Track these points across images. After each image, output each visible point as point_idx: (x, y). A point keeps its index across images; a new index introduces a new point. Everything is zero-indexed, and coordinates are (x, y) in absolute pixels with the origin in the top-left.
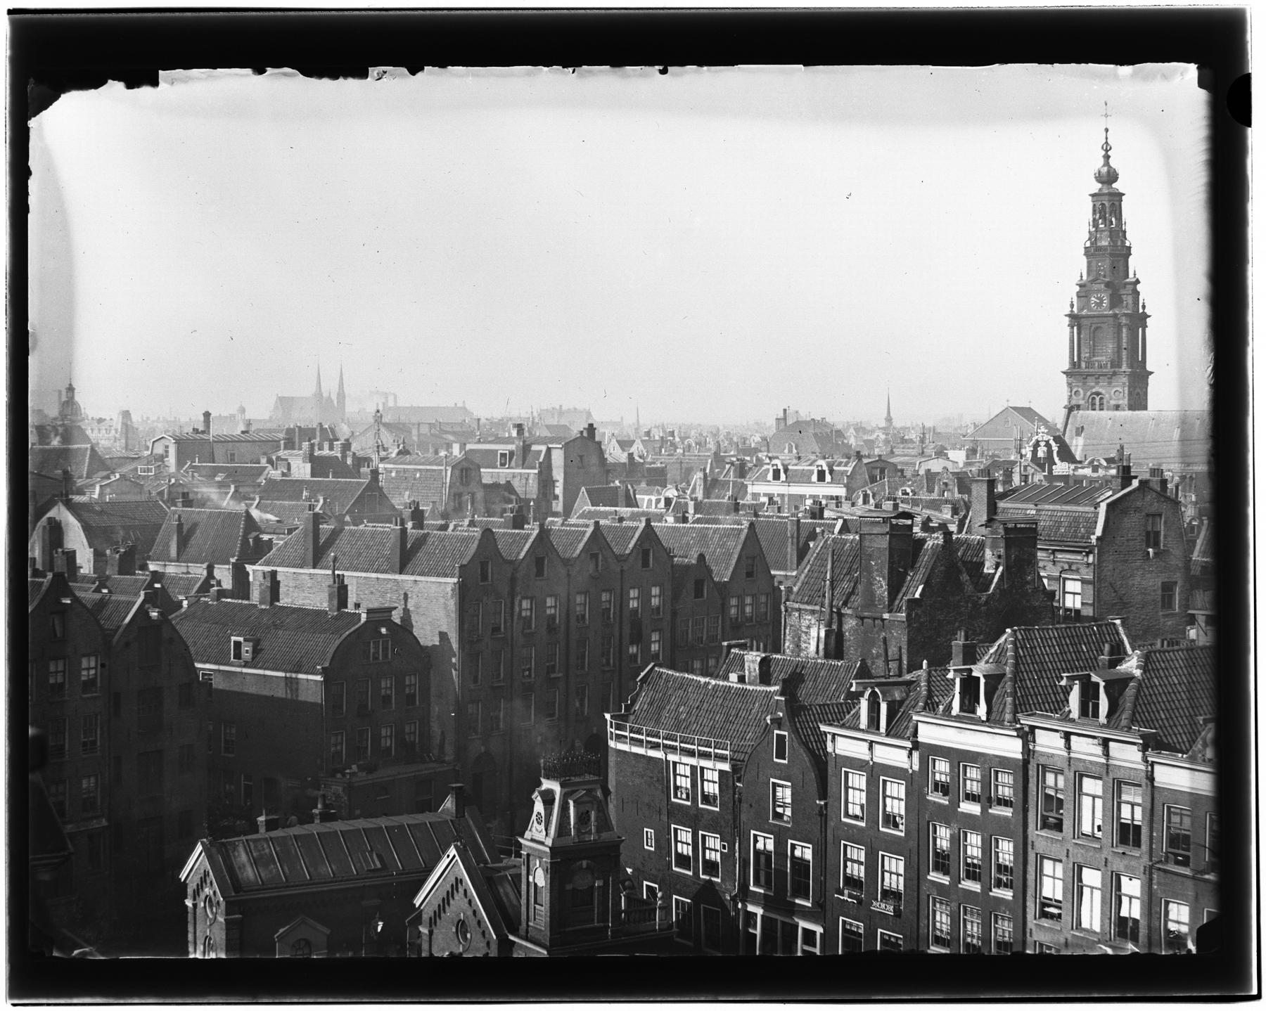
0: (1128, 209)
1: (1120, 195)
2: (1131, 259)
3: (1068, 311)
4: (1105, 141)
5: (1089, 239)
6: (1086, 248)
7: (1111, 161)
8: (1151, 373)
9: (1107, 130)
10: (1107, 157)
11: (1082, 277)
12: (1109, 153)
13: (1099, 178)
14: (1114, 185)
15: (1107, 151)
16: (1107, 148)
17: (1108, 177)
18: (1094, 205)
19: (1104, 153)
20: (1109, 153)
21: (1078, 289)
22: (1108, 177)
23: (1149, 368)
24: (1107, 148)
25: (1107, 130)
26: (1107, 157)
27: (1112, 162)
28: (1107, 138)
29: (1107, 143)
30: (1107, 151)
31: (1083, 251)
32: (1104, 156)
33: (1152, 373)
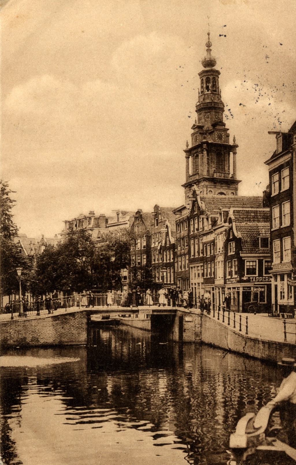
1: (218, 73)
3: (185, 148)
4: (207, 41)
5: (199, 102)
7: (212, 52)
9: (209, 34)
10: (209, 50)
11: (196, 122)
12: (211, 48)
14: (213, 68)
16: (209, 45)
17: (209, 63)
18: (202, 79)
21: (192, 131)
22: (209, 63)
24: (209, 45)
25: (209, 34)
26: (209, 50)
28: (209, 39)
29: (209, 42)
32: (207, 50)
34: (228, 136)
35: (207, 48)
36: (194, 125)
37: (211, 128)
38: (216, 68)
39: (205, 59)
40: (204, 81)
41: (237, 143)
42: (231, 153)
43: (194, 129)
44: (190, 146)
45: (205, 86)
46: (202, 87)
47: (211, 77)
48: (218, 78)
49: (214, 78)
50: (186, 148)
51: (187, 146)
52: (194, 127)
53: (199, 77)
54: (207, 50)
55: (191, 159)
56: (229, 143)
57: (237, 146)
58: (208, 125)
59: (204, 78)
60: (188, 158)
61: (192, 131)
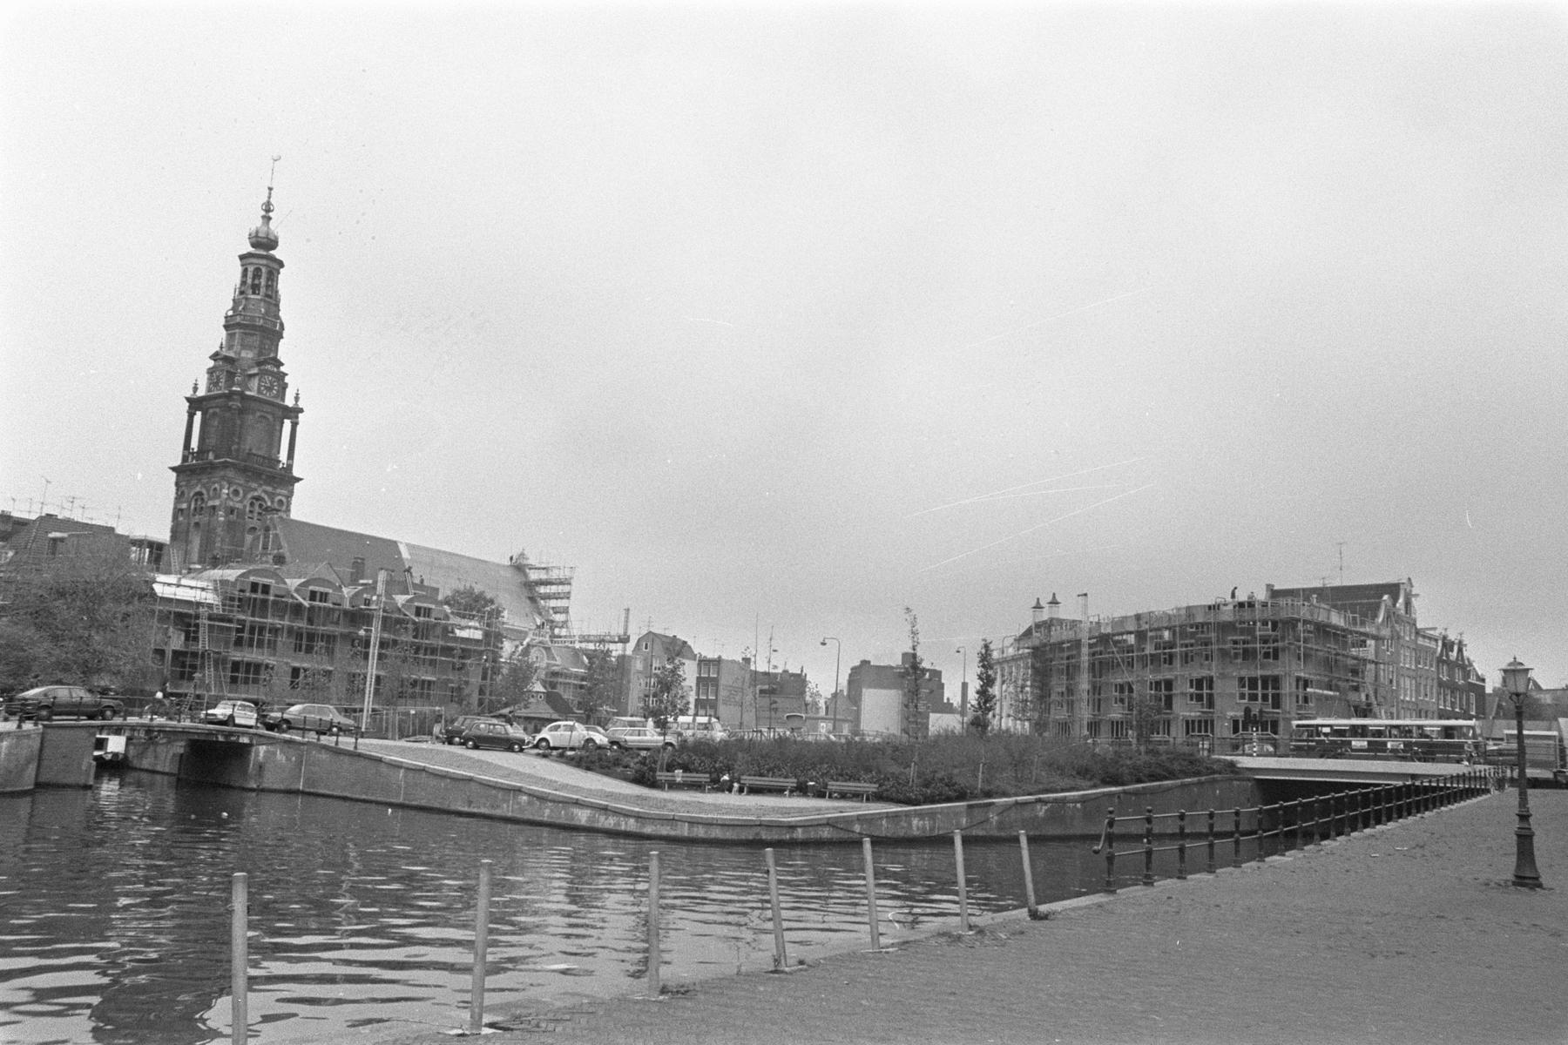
0: (286, 283)
1: (281, 264)
3: (189, 393)
4: (265, 200)
6: (226, 317)
8: (298, 480)
9: (270, 189)
10: (267, 219)
12: (271, 214)
14: (272, 252)
15: (268, 210)
16: (268, 208)
17: (264, 243)
19: (263, 213)
20: (271, 214)
21: (211, 363)
22: (264, 243)
23: (296, 473)
24: (268, 208)
25: (270, 189)
26: (267, 219)
27: (272, 225)
28: (269, 198)
31: (223, 321)
32: (263, 217)
33: (301, 479)
35: (263, 213)
36: (216, 354)
38: (276, 253)
39: (257, 232)
40: (250, 275)
41: (301, 404)
43: (215, 360)
44: (201, 392)
45: (249, 281)
46: (243, 283)
47: (264, 270)
48: (279, 273)
50: (192, 392)
51: (195, 389)
52: (215, 357)
53: (238, 262)
54: (263, 217)
55: (198, 416)
56: (283, 400)
57: (301, 411)
59: (251, 269)
60: (191, 416)
61: (211, 363)
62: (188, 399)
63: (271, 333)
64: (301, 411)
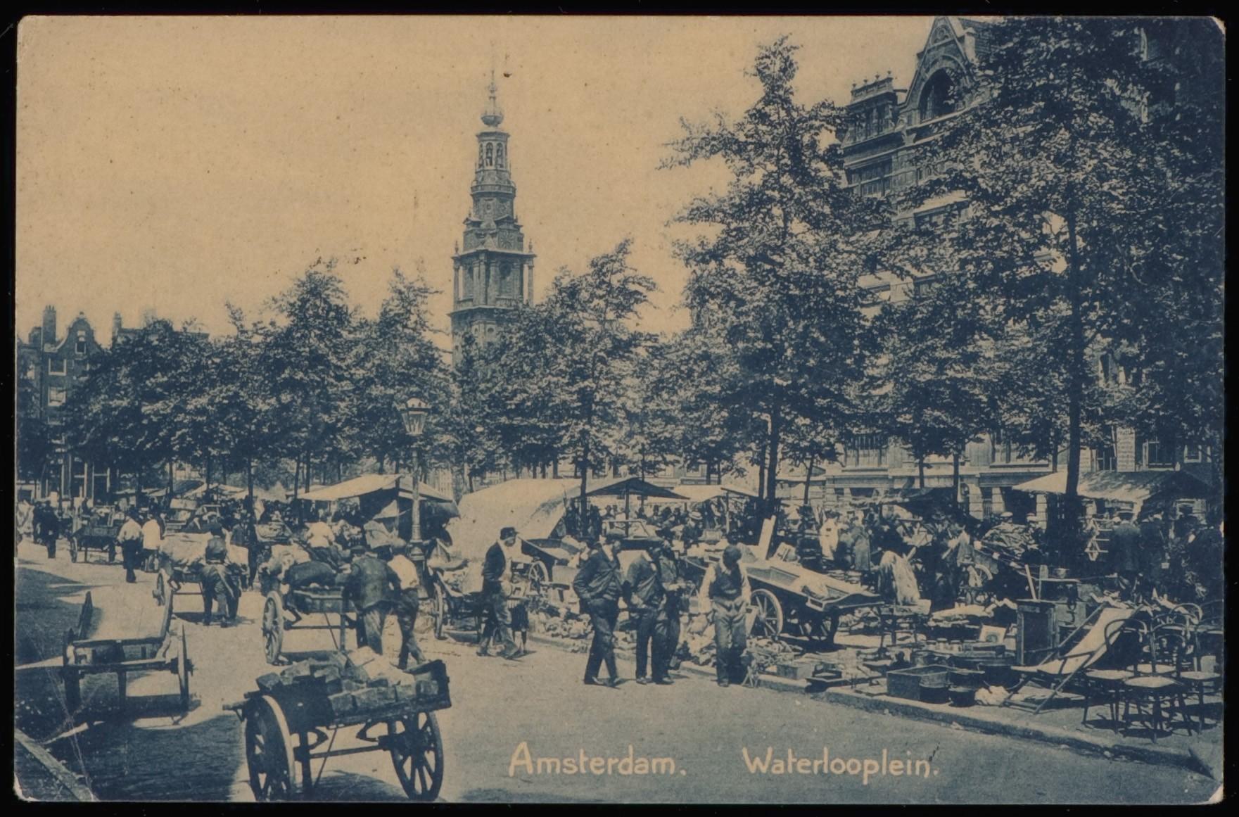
1: (507, 135)
2: (516, 201)
3: (453, 254)
13: (487, 121)
14: (499, 126)
15: (492, 91)
30: (492, 91)
34: (520, 240)
35: (490, 94)
36: (467, 219)
37: (493, 225)
38: (504, 127)
40: (484, 149)
41: (534, 251)
42: (526, 267)
44: (461, 252)
45: (484, 156)
46: (481, 158)
47: (495, 144)
49: (499, 145)
51: (457, 250)
57: (535, 256)
58: (488, 221)
59: (485, 144)
60: (457, 270)
62: (453, 258)
63: (506, 195)
64: (535, 256)
